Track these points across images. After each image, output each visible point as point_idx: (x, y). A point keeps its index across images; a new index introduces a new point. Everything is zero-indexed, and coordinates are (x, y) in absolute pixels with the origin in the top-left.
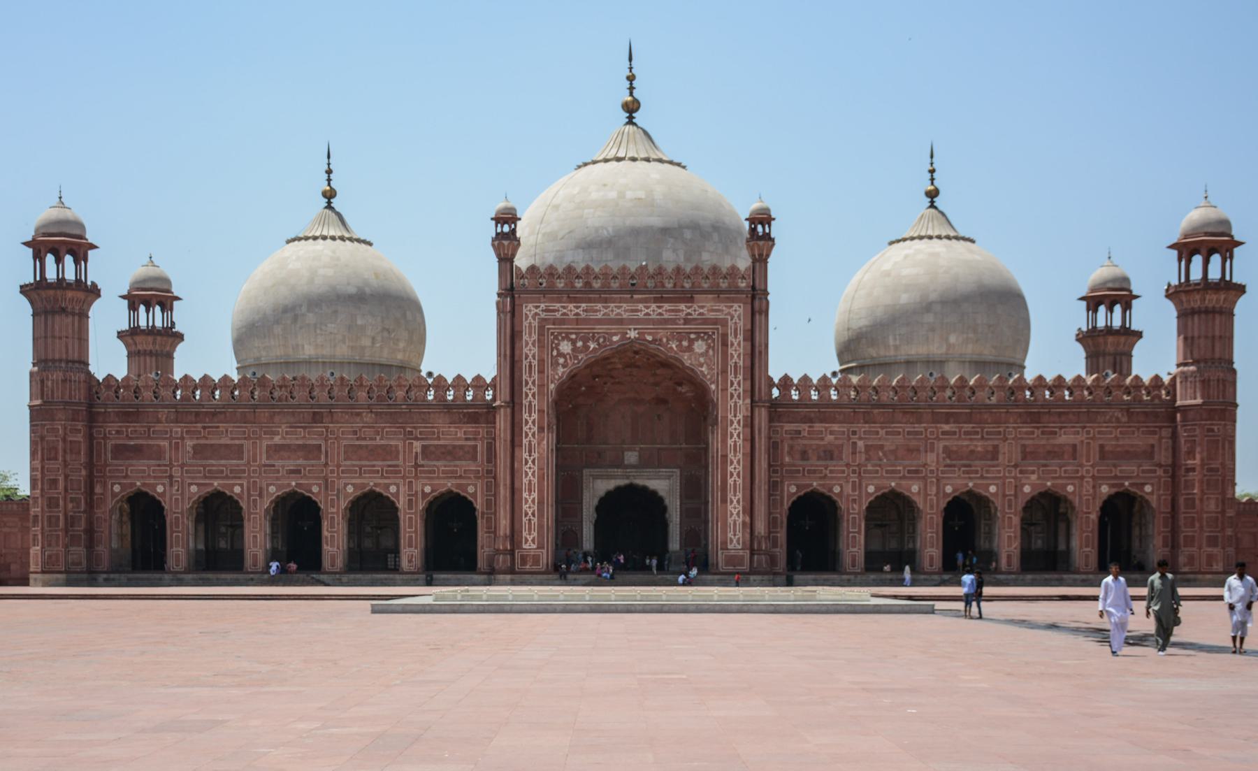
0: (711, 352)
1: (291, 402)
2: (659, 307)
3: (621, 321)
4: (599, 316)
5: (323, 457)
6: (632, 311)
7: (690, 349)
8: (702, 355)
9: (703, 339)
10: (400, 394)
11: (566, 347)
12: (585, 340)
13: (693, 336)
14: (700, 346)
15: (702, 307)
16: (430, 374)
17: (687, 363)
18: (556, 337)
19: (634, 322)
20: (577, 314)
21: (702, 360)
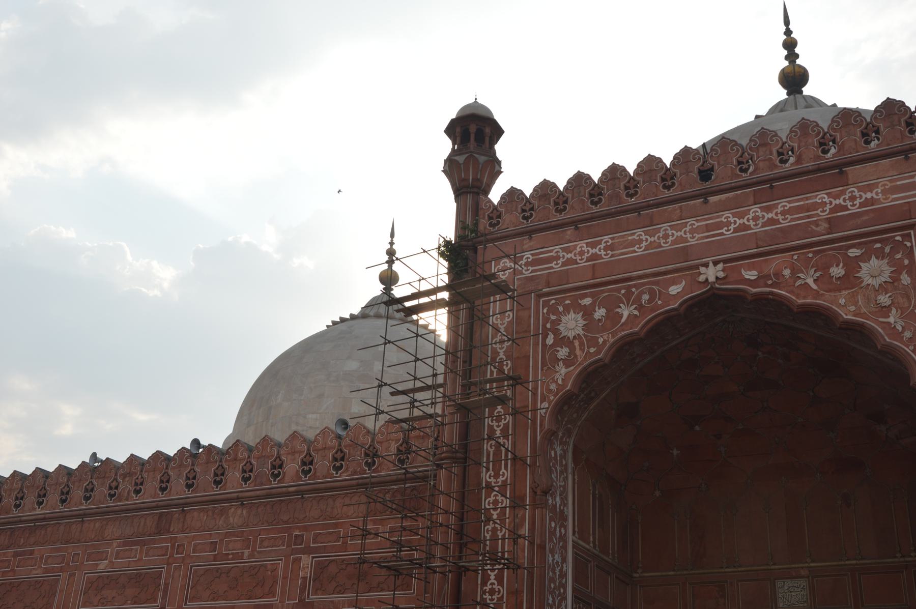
0: (905, 279)
1: (135, 500)
2: (768, 209)
3: (685, 253)
4: (639, 251)
5: (160, 594)
6: (708, 228)
7: (850, 280)
8: (883, 288)
9: (880, 255)
10: (292, 467)
11: (572, 324)
12: (611, 305)
13: (854, 252)
14: (874, 271)
15: (870, 188)
16: (344, 424)
17: (847, 315)
18: (553, 310)
19: (710, 249)
20: (595, 257)
21: (884, 299)
